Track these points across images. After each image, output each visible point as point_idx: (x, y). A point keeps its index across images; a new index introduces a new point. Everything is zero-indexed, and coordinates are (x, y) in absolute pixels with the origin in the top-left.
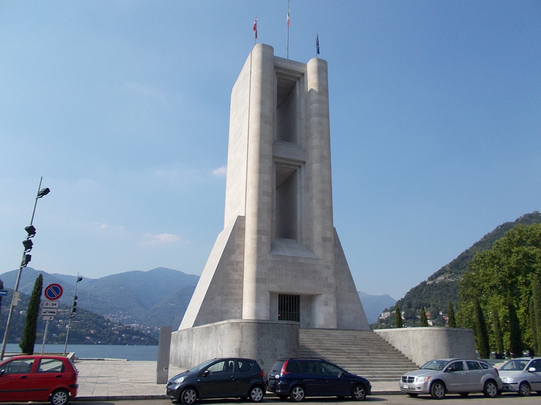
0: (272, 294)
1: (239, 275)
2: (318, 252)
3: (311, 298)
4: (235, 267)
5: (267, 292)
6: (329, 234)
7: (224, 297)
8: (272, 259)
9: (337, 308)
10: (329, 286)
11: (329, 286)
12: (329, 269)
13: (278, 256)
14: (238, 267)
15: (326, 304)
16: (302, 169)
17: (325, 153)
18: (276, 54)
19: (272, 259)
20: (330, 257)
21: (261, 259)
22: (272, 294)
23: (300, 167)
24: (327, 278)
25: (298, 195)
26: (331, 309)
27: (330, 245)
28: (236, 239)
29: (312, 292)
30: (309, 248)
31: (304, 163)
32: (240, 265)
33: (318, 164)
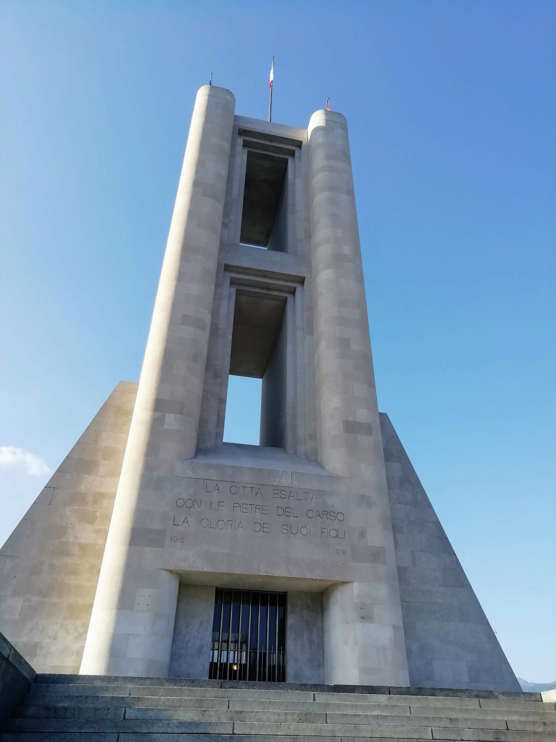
1: (97, 532)
2: (335, 459)
3: (319, 600)
4: (90, 508)
5: (165, 577)
6: (362, 415)
7: (35, 599)
8: (190, 473)
9: (408, 630)
10: (376, 555)
11: (376, 555)
12: (370, 505)
14: (93, 508)
15: (365, 616)
16: (298, 294)
17: (347, 250)
18: (239, 111)
19: (190, 473)
20: (370, 473)
22: (187, 586)
23: (293, 292)
24: (363, 534)
25: (289, 348)
26: (384, 632)
27: (370, 442)
28: (104, 435)
30: (314, 459)
31: (302, 281)
32: (105, 503)
33: (328, 271)
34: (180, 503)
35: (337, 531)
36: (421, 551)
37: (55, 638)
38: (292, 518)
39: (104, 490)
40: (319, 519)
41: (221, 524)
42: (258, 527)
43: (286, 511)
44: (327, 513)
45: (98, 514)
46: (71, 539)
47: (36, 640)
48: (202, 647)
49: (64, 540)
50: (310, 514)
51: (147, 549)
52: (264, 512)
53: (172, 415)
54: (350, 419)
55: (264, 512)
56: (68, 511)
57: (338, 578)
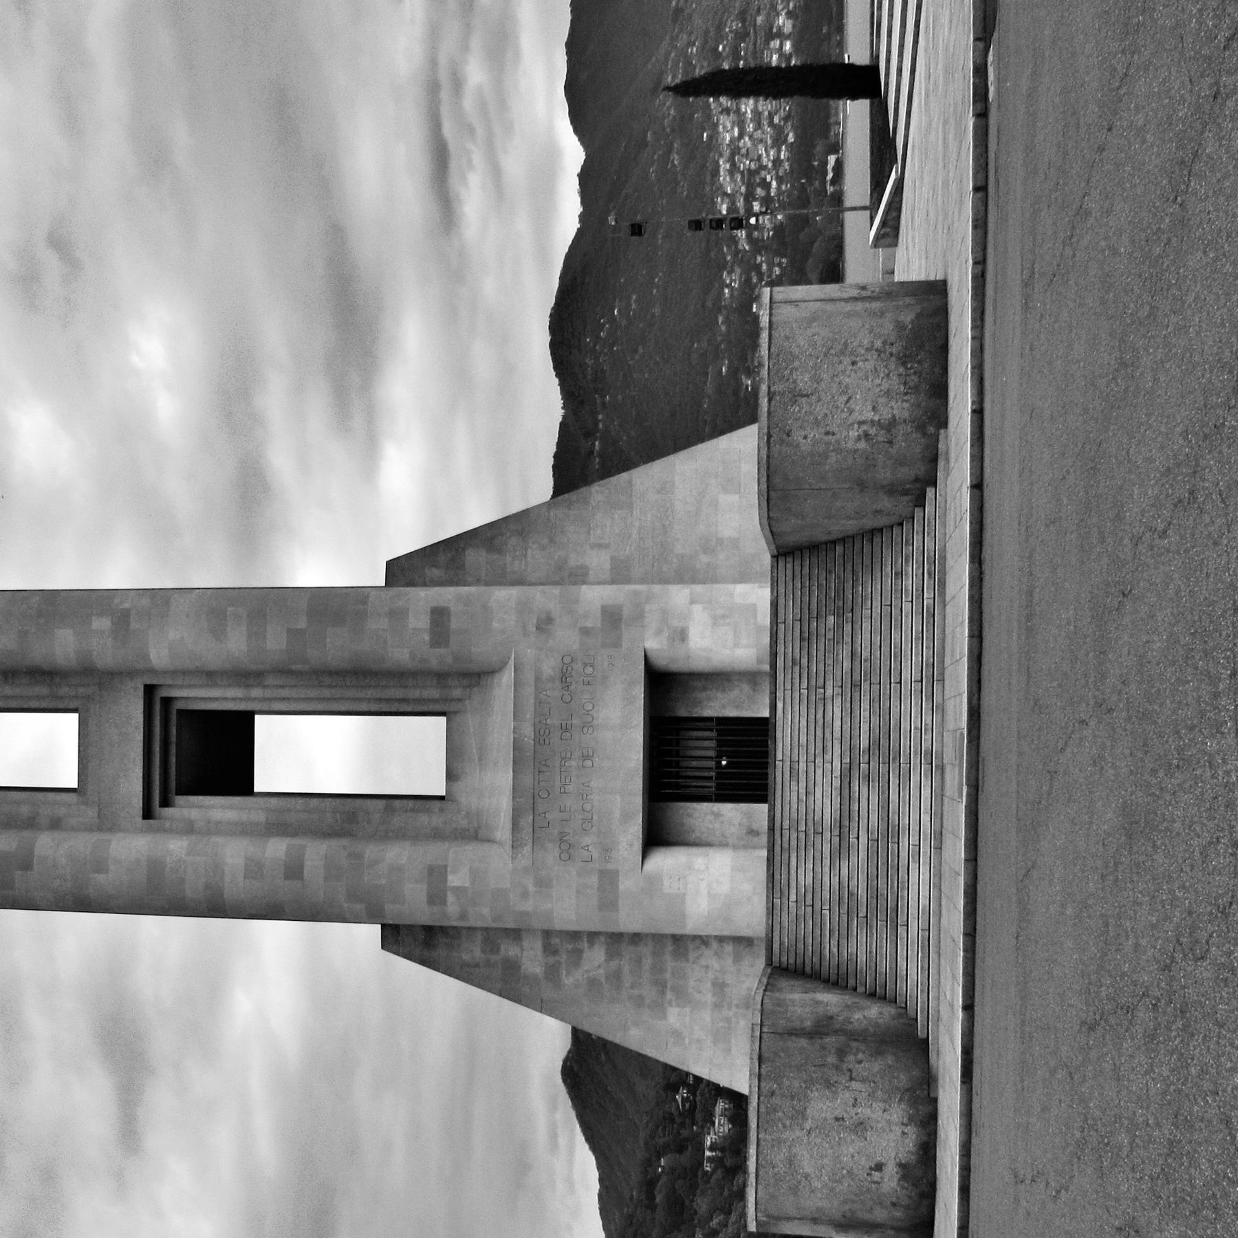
0: (656, 836)
3: (662, 684)
8: (527, 849)
13: (515, 826)
19: (527, 849)
21: (531, 888)
24: (585, 632)
28: (466, 957)
29: (639, 692)
34: (565, 856)
35: (585, 665)
36: (589, 533)
37: (707, 967)
38: (575, 721)
39: (596, 946)
40: (572, 687)
41: (588, 807)
42: (588, 763)
43: (565, 729)
44: (564, 677)
45: (570, 947)
46: (601, 971)
47: (709, 985)
48: (713, 813)
49: (603, 980)
50: (567, 698)
51: (621, 888)
52: (568, 755)
53: (450, 878)
54: (427, 638)
55: (568, 755)
56: (568, 981)
57: (642, 667)
